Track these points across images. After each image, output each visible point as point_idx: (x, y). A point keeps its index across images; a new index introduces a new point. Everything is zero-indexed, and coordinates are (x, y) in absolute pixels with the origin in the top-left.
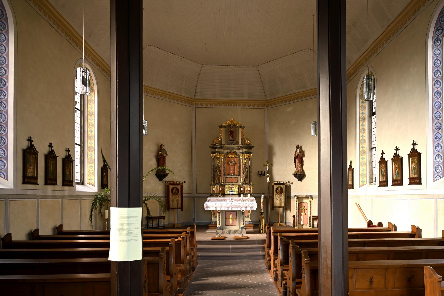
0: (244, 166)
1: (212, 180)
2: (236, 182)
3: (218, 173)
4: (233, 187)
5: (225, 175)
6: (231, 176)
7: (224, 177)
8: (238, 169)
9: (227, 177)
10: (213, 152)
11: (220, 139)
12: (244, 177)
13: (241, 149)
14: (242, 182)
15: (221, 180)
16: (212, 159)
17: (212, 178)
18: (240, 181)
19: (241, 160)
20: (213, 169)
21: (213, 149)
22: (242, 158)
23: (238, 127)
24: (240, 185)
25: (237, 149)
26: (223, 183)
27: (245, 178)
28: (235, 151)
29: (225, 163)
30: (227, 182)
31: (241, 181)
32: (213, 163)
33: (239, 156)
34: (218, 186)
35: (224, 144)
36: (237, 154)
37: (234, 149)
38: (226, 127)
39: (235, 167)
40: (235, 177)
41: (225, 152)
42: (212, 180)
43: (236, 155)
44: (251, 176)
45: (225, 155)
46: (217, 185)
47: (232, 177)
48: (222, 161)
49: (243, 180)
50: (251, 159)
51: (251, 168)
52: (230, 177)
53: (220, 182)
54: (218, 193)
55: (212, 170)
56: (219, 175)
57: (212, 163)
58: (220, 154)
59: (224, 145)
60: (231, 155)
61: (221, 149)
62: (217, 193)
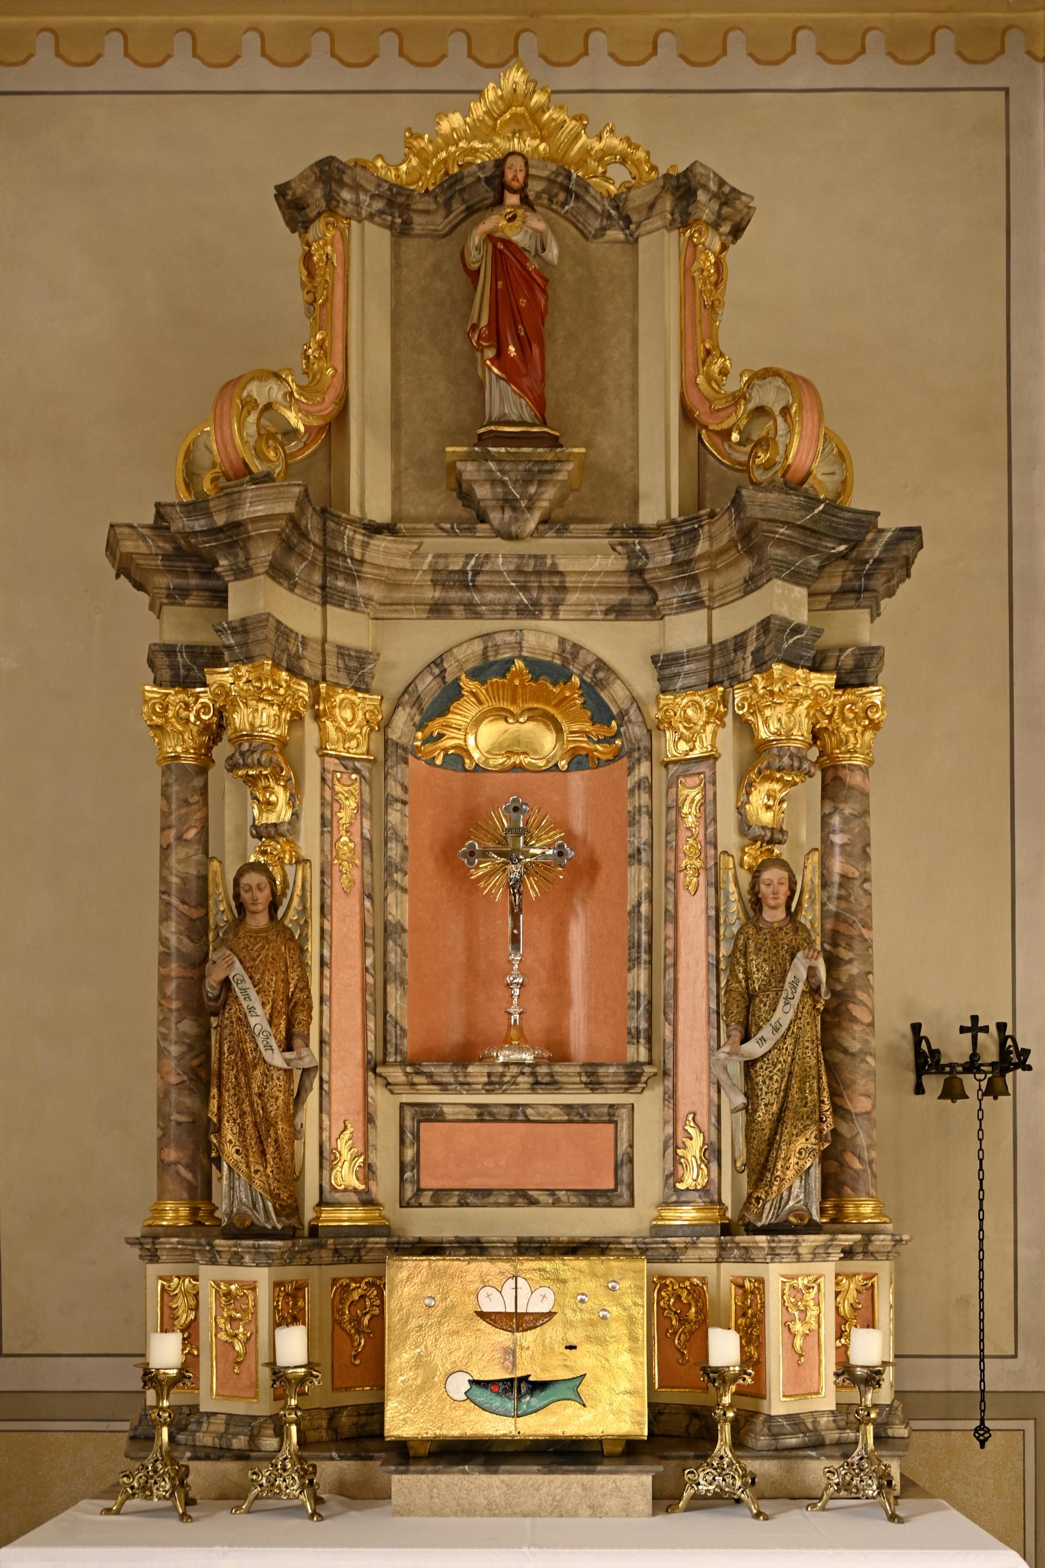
0: (756, 902)
1: (172, 1155)
2: (592, 1198)
3: (258, 1021)
4: (537, 1303)
5: (396, 1074)
6: (493, 1085)
7: (386, 1105)
8: (634, 962)
9: (430, 1114)
10: (170, 650)
11: (293, 418)
12: (751, 1094)
13: (697, 603)
14: (709, 1195)
15: (326, 1158)
16: (165, 796)
17: (163, 1116)
18: (672, 1177)
19: (691, 794)
20: (174, 968)
21: (178, 595)
22: (712, 758)
23: (638, 198)
24: (674, 1255)
25: (620, 612)
26: (348, 1216)
27: (779, 1120)
28: (577, 648)
29: (395, 850)
30: (439, 1198)
31: (692, 1178)
32: (193, 851)
33: (655, 729)
34: (262, 1276)
35: (380, 511)
36: (615, 696)
37: (555, 616)
38: (405, 209)
39: (577, 934)
40: (577, 1114)
41: (387, 655)
42: (163, 1166)
43: (601, 713)
44: (862, 1083)
45: (402, 720)
46: (236, 1260)
47: (516, 1114)
48: (344, 816)
49: (712, 1153)
50: (856, 779)
51: (867, 944)
52: (484, 1114)
53: (311, 1197)
54: (262, 1407)
55: (163, 980)
56: (277, 1058)
57: (165, 850)
58: (295, 672)
59: (374, 529)
60: (503, 714)
61: (328, 597)
62: (239, 1408)
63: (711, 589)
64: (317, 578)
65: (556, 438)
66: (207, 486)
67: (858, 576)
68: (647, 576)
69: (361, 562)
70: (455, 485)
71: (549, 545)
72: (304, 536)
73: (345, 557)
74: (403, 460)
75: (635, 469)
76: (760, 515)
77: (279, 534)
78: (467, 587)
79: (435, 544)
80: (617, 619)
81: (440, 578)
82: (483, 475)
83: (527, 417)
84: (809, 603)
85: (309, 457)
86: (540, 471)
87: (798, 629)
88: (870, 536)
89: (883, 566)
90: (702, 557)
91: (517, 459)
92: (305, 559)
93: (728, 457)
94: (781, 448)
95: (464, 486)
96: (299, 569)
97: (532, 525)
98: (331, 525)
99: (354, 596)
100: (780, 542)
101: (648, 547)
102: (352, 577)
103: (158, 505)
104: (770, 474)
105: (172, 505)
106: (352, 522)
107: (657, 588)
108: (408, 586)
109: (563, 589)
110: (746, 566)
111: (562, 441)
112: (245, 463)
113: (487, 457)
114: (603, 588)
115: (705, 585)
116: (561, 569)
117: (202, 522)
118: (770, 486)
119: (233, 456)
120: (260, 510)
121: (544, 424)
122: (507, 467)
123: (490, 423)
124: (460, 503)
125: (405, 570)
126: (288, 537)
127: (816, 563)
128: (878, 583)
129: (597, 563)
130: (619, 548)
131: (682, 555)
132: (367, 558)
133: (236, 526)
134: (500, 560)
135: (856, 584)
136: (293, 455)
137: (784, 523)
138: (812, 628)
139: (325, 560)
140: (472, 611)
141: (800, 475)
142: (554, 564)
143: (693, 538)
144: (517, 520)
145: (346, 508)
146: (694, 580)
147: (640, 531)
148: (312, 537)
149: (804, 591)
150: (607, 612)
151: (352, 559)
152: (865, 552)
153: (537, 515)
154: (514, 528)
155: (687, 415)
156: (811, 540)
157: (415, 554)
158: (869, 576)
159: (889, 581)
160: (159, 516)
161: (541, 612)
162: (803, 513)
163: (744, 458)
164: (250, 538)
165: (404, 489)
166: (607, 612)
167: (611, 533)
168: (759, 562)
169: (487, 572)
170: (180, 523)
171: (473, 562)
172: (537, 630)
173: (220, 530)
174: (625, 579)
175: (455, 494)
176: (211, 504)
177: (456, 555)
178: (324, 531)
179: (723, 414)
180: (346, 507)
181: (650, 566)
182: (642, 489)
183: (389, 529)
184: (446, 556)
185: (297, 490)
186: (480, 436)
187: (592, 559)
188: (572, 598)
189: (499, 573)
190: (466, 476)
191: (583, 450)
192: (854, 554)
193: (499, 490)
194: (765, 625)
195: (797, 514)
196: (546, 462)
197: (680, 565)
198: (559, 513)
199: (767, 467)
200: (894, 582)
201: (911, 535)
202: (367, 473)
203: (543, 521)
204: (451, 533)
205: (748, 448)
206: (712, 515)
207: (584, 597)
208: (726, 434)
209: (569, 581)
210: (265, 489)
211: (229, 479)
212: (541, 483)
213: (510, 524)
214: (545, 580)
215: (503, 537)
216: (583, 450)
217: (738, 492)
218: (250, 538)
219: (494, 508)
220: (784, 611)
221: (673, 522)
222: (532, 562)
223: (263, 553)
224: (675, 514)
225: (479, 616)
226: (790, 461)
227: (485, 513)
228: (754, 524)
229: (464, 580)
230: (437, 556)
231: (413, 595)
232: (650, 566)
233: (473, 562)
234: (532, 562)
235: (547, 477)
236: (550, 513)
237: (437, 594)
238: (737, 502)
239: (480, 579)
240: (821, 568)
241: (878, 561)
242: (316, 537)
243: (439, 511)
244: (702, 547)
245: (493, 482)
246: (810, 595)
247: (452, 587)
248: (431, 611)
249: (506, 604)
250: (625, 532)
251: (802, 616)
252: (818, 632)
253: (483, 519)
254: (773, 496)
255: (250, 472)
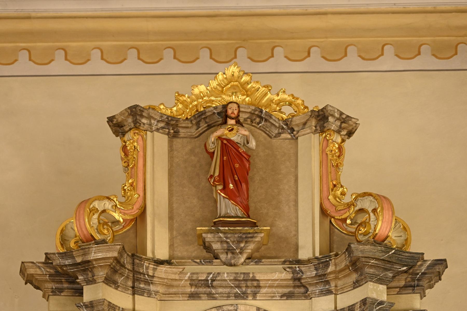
13: (329, 292)
35: (162, 254)
37: (254, 297)
63: (336, 286)
64: (130, 283)
65: (255, 223)
66: (72, 245)
67: (413, 280)
68: (302, 281)
69: (153, 277)
70: (201, 243)
71: (251, 268)
72: (123, 266)
73: (145, 274)
74: (175, 233)
75: (296, 235)
76: (361, 255)
77: (110, 265)
78: (209, 287)
79: (190, 269)
80: (287, 299)
81: (193, 283)
82: (217, 239)
83: (240, 215)
84: (387, 292)
85: (125, 232)
86: (246, 237)
87: (381, 303)
88: (419, 263)
89: (427, 276)
90: (330, 273)
91: (234, 232)
92: (123, 276)
93: (346, 230)
94: (372, 227)
95: (207, 244)
96: (120, 280)
97: (242, 260)
98: (137, 261)
99: (149, 291)
100: (372, 266)
101: (303, 269)
102: (148, 283)
103: (46, 254)
104: (366, 237)
105: (54, 254)
106: (148, 259)
107: (308, 286)
108: (177, 286)
109: (259, 287)
110: (354, 276)
111: (257, 224)
112: (92, 235)
113: (218, 231)
114: (279, 286)
115: (333, 284)
116: (257, 278)
117: (69, 261)
118: (367, 242)
119: (85, 232)
120: (100, 255)
121: (249, 217)
122: (229, 236)
123: (220, 217)
124: (205, 251)
125: (176, 280)
126: (114, 267)
127: (391, 275)
128: (424, 283)
129: (276, 276)
130: (288, 269)
131: (320, 272)
132: (156, 275)
133: (89, 261)
134: (226, 275)
135: (413, 283)
136: (117, 231)
137: (373, 258)
138: (389, 302)
139: (134, 276)
140: (211, 296)
141: (383, 238)
142: (253, 276)
143: (327, 265)
144: (234, 258)
145: (145, 254)
146: (327, 282)
147: (299, 262)
148: (127, 266)
149: (385, 287)
150: (281, 297)
151: (148, 275)
152: (417, 270)
153: (245, 256)
154: (233, 261)
155: (323, 212)
156: (388, 265)
157: (181, 273)
158: (419, 280)
159: (430, 282)
160: (47, 258)
161: (247, 297)
162: (384, 254)
163: (353, 230)
164: (94, 267)
165: (175, 245)
166: (281, 297)
167: (284, 263)
168: (361, 275)
169: (219, 280)
170: (58, 261)
171: (211, 276)
172: (245, 304)
173: (79, 264)
174: (291, 282)
175: (202, 247)
176: (74, 253)
177: (202, 273)
178: (133, 264)
179: (342, 212)
180: (144, 252)
181: (303, 277)
182: (301, 243)
183: (168, 262)
184: (197, 273)
185: (119, 247)
186: (215, 223)
187: (273, 274)
188: (264, 291)
189: (226, 280)
190: (207, 240)
191: (269, 228)
192: (411, 271)
193: (225, 245)
194: (364, 302)
195: (380, 254)
196: (249, 233)
197: (320, 276)
198: (256, 254)
199: (365, 234)
200: (433, 282)
201: (442, 263)
202: (156, 238)
203: (248, 258)
204: (200, 264)
205: (356, 226)
206: (336, 255)
207: (270, 290)
208: (344, 220)
209: (262, 283)
210: (101, 246)
211: (83, 242)
212: (246, 242)
213: (231, 259)
214: (249, 283)
215: (227, 265)
216: (269, 228)
217: (349, 246)
218: (94, 267)
219: (222, 253)
220: (374, 296)
221: (317, 258)
222: (242, 276)
223: (101, 274)
224: (317, 254)
225: (215, 299)
226: (377, 232)
227: (218, 255)
228: (358, 259)
229: (206, 283)
230: (193, 274)
231: (180, 290)
232: (303, 277)
233: (211, 276)
234: (242, 276)
235: (250, 239)
236: (252, 255)
237: (193, 290)
238: (349, 250)
239: (215, 283)
240: (394, 277)
241: (424, 274)
242: (129, 267)
243: (194, 254)
244: (331, 268)
245: (222, 242)
246: (388, 288)
247: (200, 287)
248: (189, 297)
249: (229, 293)
250: (291, 263)
251: (384, 297)
252: (392, 304)
253: (217, 257)
254: (367, 247)
255: (95, 239)
